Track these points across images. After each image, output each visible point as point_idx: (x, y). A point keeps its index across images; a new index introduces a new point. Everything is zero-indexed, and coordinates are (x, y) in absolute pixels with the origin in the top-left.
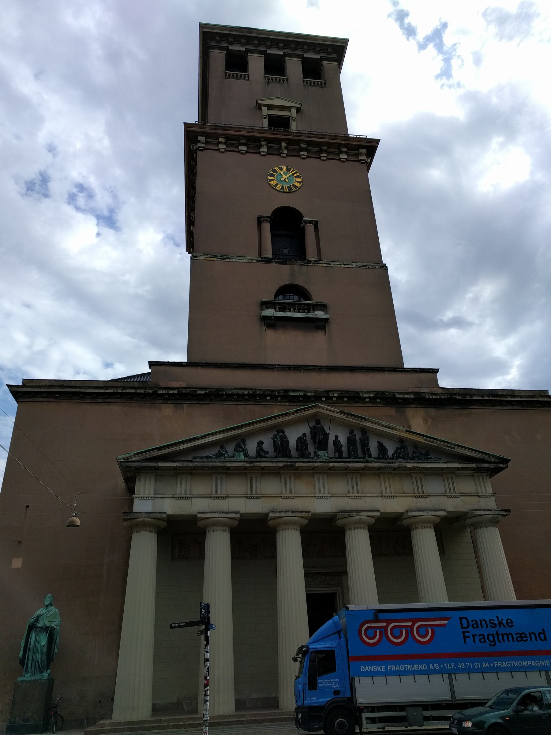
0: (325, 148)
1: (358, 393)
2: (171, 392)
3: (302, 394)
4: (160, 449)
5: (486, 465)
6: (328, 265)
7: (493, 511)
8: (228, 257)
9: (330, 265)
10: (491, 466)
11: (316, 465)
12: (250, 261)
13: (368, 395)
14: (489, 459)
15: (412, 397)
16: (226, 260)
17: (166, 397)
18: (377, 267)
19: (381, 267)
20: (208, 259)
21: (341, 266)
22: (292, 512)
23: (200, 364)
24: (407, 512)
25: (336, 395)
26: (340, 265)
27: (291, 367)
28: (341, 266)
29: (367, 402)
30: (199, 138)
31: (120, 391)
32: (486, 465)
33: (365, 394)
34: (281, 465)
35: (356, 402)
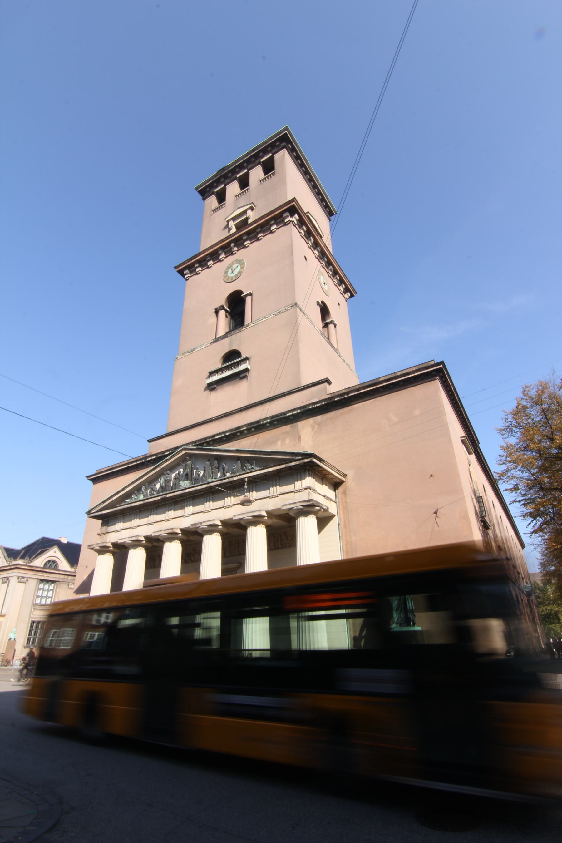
0: (259, 230)
1: (258, 421)
2: (153, 458)
3: (223, 435)
4: (104, 502)
5: (293, 464)
6: (254, 324)
7: (297, 503)
8: (195, 349)
9: (255, 324)
10: (298, 463)
11: (178, 493)
12: (207, 346)
13: (266, 421)
14: (297, 458)
15: (299, 411)
16: (194, 352)
17: (152, 461)
18: (289, 308)
19: (291, 307)
20: (183, 356)
21: (263, 320)
22: (164, 530)
23: (172, 433)
24: (235, 516)
25: (244, 428)
26: (262, 320)
27: (222, 415)
28: (263, 320)
29: (269, 427)
30: (185, 272)
31: (130, 465)
32: (293, 464)
33: (264, 421)
34: (159, 498)
35: (261, 429)
